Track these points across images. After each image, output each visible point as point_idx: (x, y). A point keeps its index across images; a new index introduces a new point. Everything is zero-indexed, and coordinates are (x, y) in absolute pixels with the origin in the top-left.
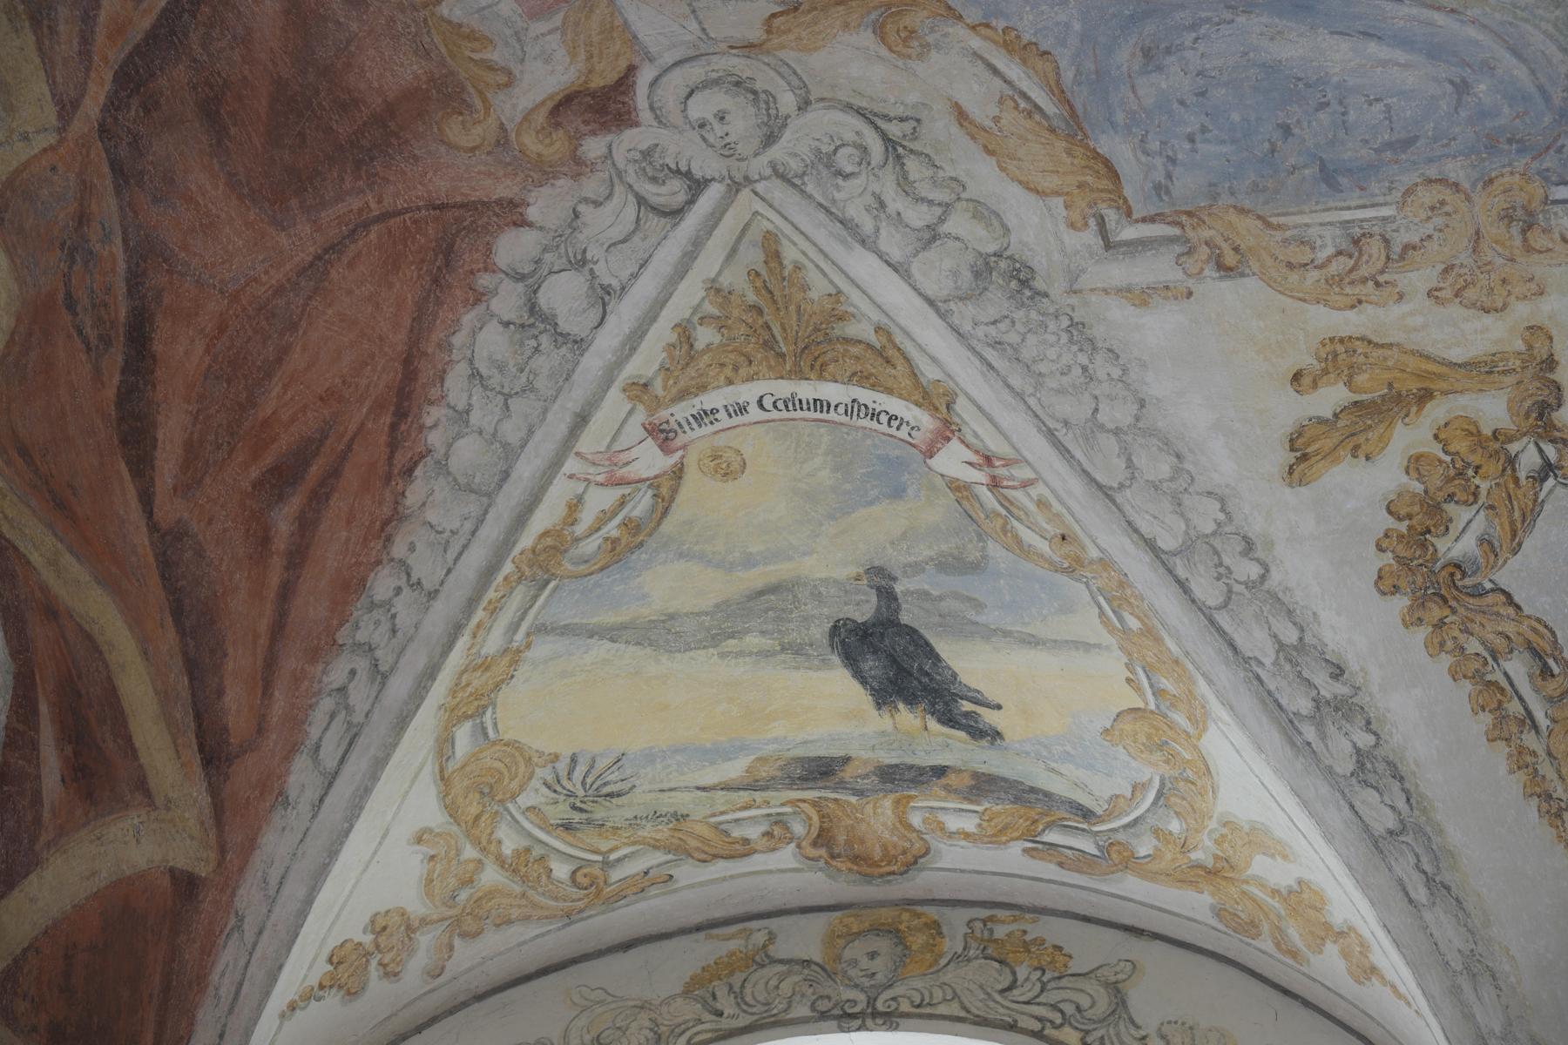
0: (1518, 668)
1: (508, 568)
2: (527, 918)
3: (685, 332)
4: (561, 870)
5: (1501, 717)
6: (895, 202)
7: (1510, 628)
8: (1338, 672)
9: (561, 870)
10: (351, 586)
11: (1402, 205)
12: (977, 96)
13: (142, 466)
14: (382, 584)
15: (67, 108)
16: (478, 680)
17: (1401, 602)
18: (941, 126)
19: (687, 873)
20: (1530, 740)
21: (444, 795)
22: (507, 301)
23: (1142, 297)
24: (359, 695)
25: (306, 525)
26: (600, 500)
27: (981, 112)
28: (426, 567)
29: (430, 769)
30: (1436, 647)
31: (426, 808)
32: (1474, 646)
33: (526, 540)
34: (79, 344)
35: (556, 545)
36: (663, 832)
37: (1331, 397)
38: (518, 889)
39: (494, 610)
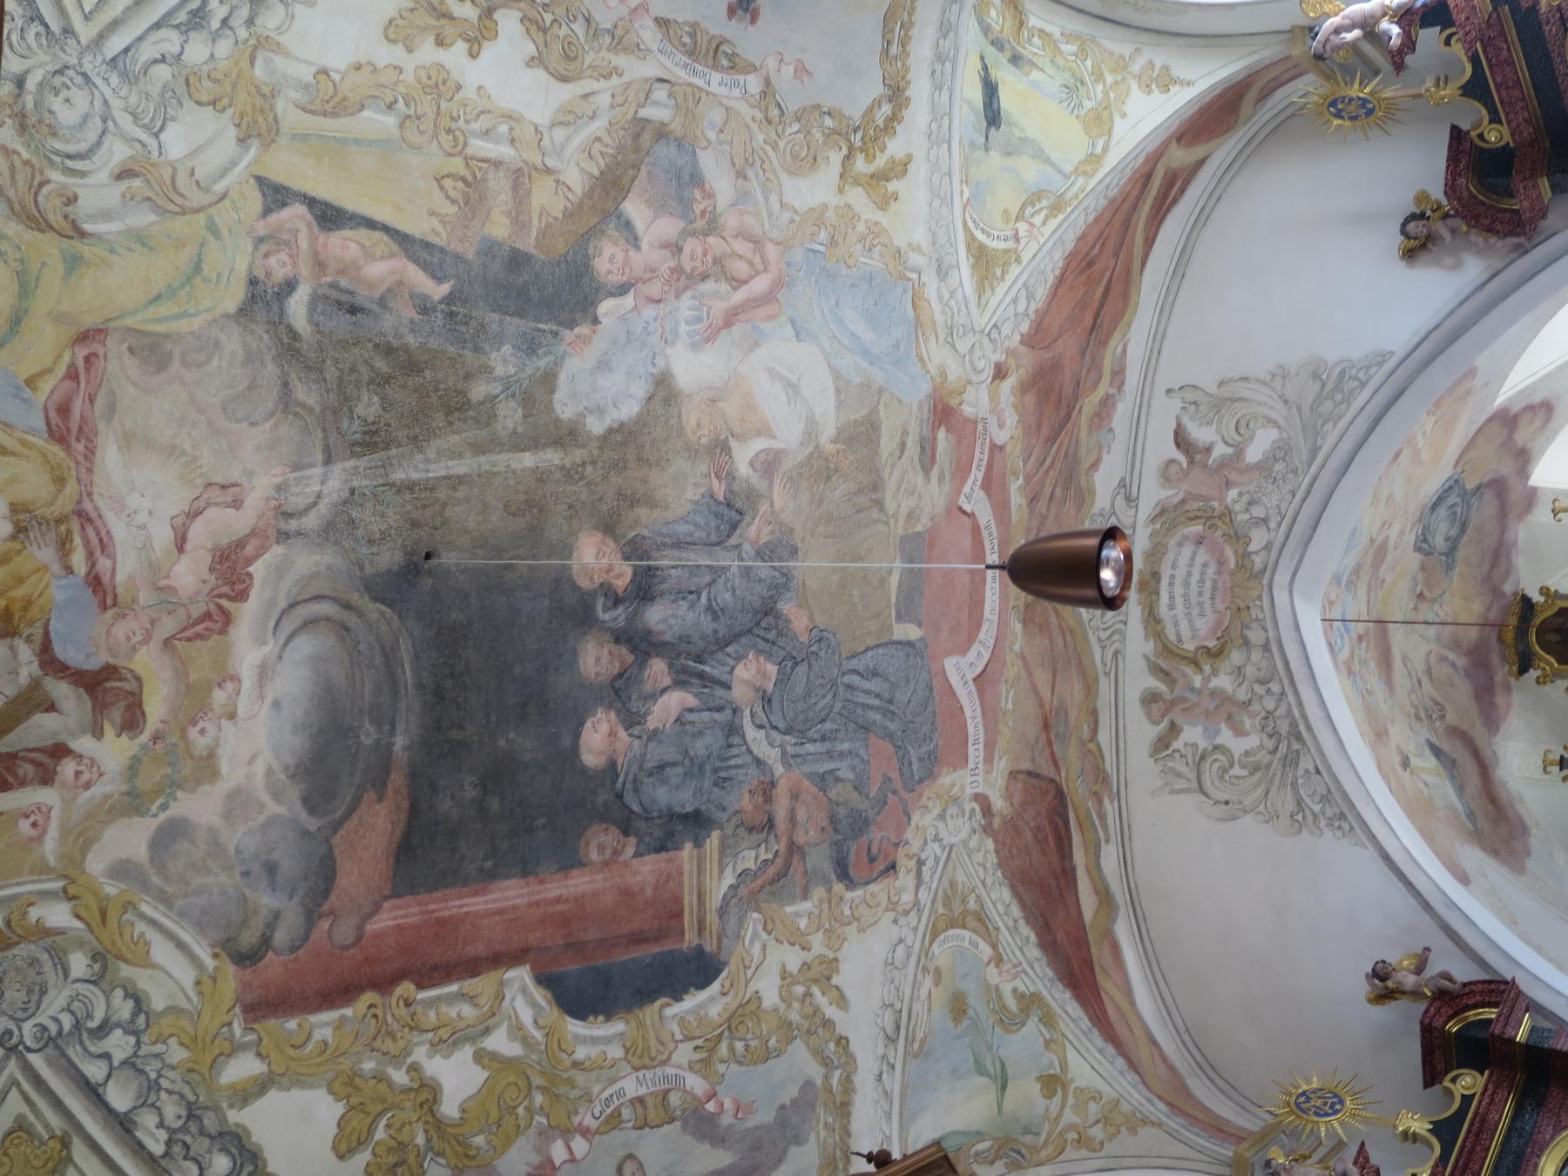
0: (894, 50)
1: (1069, 210)
2: (1105, 50)
3: (1003, 279)
4: (1089, 63)
5: (907, 31)
6: (956, 310)
7: (889, 68)
8: (934, 72)
9: (1089, 63)
10: (1097, 219)
11: (858, 261)
12: (933, 345)
13: (1109, 282)
14: (1091, 218)
15: (1080, 411)
16: (1088, 168)
17: (908, 93)
18: (942, 336)
19: (1056, 32)
20: (906, 18)
21: (1111, 128)
22: (1033, 307)
23: (917, 249)
24: (1115, 182)
25: (1093, 246)
26: (1038, 220)
27: (933, 338)
28: (1083, 217)
29: (1114, 141)
30: (907, 69)
31: (1120, 127)
32: (900, 64)
33: (1061, 217)
34: (1088, 318)
35: (1055, 209)
36: (1058, 58)
37: (892, 186)
38: (1103, 66)
39: (1076, 195)
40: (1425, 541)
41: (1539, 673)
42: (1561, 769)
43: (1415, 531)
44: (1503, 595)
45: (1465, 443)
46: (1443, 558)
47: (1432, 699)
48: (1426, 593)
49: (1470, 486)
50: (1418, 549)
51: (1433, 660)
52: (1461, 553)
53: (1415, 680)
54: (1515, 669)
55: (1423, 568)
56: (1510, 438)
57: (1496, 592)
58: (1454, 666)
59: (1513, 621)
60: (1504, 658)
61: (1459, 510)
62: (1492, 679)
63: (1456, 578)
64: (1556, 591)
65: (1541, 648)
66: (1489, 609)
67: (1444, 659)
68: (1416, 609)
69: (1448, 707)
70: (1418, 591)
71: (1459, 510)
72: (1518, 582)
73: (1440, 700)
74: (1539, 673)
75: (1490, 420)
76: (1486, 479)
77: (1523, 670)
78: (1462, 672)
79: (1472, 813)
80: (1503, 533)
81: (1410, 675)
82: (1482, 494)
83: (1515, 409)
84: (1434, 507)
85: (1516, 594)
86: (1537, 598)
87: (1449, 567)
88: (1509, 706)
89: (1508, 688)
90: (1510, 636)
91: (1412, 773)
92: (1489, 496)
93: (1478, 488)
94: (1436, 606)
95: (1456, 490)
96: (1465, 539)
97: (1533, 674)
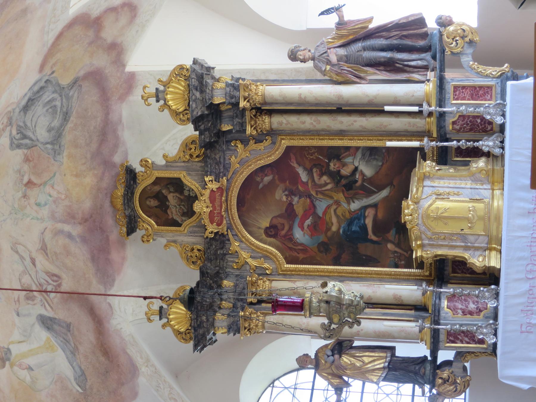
40: (25, 137)
41: (143, 232)
42: (161, 319)
43: (7, 133)
44: (114, 165)
45: (46, 50)
46: (49, 146)
47: (47, 273)
48: (34, 179)
49: (65, 81)
50: (19, 146)
51: (48, 236)
52: (67, 138)
53: (28, 261)
54: (125, 229)
55: (27, 160)
56: (98, 37)
57: (107, 164)
58: (70, 236)
59: (120, 191)
60: (116, 221)
61: (58, 103)
62: (107, 238)
63: (65, 160)
64: (153, 163)
65: (143, 212)
66: (101, 179)
67: (58, 233)
68: (25, 196)
69: (64, 276)
70: (26, 180)
71: (58, 103)
72: (126, 154)
73: (56, 271)
74: (143, 232)
75: (71, 25)
76: (82, 73)
77: (131, 229)
78: (78, 240)
79: (83, 373)
80: (107, 114)
81: (22, 258)
82: (80, 86)
83: (95, 13)
84: (26, 109)
85: (122, 165)
86: (139, 169)
87: (56, 153)
88: (124, 259)
89: (123, 245)
90: (119, 202)
91: (12, 366)
92: (86, 86)
93: (75, 82)
94: (48, 189)
95: (50, 88)
96: (70, 125)
97: (139, 233)
